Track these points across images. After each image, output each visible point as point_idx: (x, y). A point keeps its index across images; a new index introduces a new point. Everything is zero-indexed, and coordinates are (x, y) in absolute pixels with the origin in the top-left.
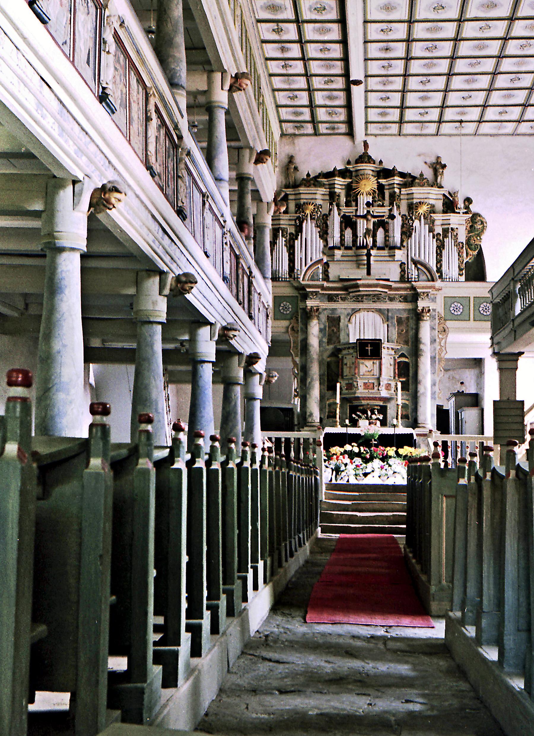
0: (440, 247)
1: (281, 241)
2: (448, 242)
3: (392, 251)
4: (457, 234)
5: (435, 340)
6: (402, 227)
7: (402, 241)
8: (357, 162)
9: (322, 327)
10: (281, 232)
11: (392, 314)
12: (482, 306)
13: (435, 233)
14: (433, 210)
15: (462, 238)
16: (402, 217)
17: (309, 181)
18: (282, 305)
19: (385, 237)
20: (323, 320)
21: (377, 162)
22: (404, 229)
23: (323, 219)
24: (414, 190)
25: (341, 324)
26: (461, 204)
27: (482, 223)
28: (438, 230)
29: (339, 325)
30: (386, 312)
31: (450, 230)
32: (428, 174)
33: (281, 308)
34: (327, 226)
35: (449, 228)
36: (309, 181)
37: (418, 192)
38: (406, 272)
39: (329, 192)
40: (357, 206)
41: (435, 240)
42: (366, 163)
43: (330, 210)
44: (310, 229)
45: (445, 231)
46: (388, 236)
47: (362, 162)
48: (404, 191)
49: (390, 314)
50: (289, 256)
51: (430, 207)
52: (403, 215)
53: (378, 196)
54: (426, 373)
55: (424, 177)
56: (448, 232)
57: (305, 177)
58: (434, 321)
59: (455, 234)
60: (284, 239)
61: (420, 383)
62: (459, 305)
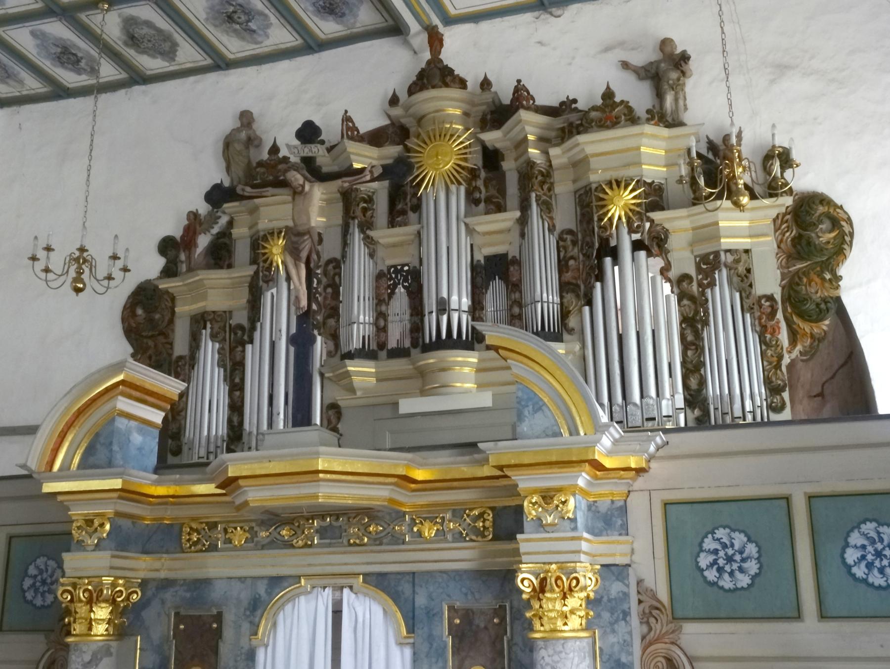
1: (209, 351)
2: (722, 298)
4: (749, 271)
7: (564, 314)
8: (411, 91)
10: (209, 325)
11: (430, 598)
12: (855, 538)
14: (655, 197)
15: (768, 280)
16: (561, 239)
18: (32, 571)
19: (510, 308)
21: (473, 79)
22: (568, 276)
23: (325, 273)
24: (591, 143)
27: (835, 223)
28: (684, 261)
29: (216, 651)
30: (406, 588)
32: (636, 94)
33: (28, 582)
34: (336, 294)
42: (434, 87)
45: (709, 264)
47: (421, 90)
48: (554, 152)
49: (421, 600)
51: (646, 195)
52: (562, 232)
53: (486, 186)
55: (617, 99)
58: (621, 627)
59: (741, 269)
60: (217, 345)
62: (739, 539)
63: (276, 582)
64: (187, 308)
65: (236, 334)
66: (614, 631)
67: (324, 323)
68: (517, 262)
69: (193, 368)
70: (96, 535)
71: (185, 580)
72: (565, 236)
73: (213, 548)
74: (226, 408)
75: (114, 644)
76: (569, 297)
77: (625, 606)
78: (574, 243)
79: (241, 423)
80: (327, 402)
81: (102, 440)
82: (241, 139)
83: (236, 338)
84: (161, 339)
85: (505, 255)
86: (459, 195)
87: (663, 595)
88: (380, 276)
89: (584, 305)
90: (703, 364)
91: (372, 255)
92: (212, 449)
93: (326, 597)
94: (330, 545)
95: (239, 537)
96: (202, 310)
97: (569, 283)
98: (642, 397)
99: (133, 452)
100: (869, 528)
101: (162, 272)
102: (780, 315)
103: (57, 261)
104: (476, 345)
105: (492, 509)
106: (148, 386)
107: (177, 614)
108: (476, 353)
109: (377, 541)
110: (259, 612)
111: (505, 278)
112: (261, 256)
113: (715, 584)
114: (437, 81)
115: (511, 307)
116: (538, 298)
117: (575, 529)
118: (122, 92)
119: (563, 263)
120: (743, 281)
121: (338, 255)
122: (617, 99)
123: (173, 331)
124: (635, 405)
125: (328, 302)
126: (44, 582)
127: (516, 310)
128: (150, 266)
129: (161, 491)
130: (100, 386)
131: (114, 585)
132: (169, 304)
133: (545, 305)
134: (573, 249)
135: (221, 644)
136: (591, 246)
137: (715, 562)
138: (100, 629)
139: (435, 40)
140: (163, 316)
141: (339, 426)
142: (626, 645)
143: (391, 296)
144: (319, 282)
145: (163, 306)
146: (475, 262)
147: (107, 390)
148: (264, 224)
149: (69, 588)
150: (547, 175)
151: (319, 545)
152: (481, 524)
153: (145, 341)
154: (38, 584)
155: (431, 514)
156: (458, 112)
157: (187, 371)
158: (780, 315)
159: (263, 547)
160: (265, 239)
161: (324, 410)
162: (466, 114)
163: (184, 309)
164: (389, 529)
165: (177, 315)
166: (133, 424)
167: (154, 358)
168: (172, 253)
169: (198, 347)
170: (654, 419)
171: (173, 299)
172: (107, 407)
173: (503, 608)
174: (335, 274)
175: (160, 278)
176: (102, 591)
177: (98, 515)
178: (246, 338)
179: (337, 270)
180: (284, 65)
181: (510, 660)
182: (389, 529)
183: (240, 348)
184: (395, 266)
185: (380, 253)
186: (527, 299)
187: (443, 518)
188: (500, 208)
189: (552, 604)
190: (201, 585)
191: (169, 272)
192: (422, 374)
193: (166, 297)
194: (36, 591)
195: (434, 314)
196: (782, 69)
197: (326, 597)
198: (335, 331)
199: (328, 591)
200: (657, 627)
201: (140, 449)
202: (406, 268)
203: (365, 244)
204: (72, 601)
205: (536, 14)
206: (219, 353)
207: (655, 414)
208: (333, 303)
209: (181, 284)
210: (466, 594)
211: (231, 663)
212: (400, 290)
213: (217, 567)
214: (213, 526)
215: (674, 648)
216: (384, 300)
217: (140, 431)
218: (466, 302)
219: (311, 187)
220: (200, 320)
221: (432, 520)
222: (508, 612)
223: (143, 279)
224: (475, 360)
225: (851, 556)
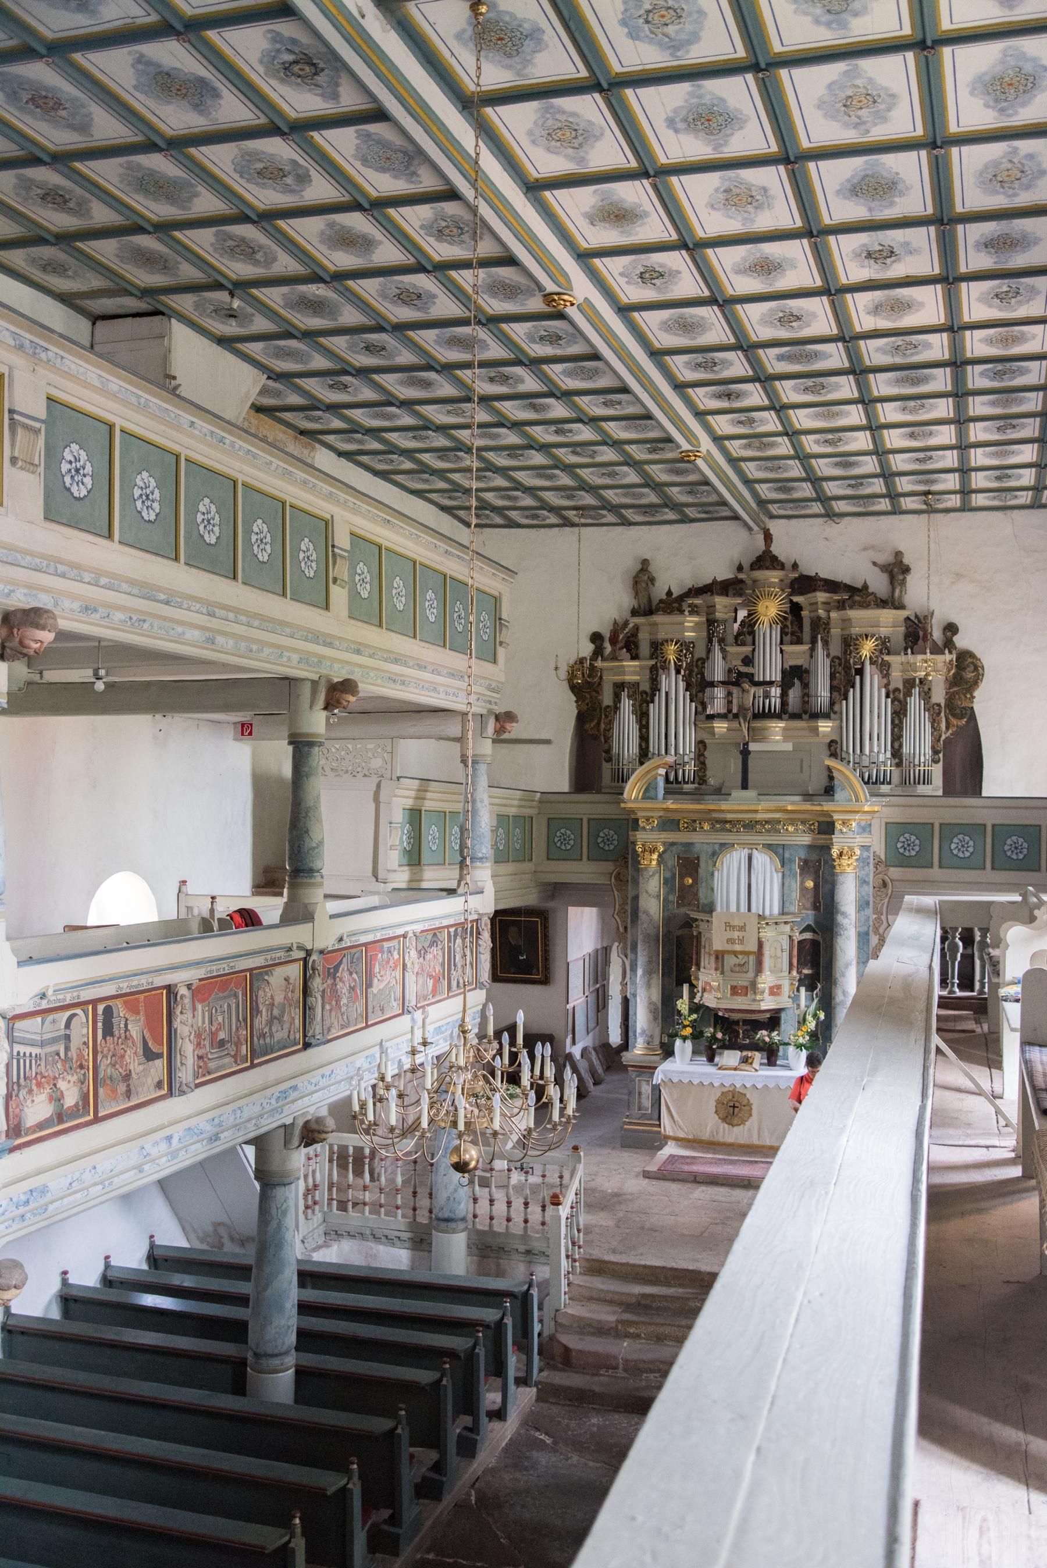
0: (899, 714)
1: (627, 705)
2: (915, 703)
3: (812, 724)
5: (868, 903)
6: (832, 676)
7: (832, 703)
9: (668, 875)
12: (955, 840)
13: (891, 687)
15: (939, 696)
16: (832, 661)
17: (670, 604)
18: (601, 834)
20: (670, 864)
22: (835, 683)
23: (697, 666)
24: (855, 614)
25: (702, 871)
26: (937, 635)
27: (976, 668)
30: (781, 851)
31: (917, 681)
33: (600, 840)
35: (914, 680)
36: (670, 604)
37: (859, 617)
39: (708, 620)
40: (754, 644)
41: (889, 700)
42: (767, 568)
43: (709, 651)
44: (672, 684)
45: (909, 684)
46: (808, 695)
47: (759, 568)
48: (834, 615)
49: (787, 855)
50: (640, 730)
52: (834, 657)
55: (870, 590)
56: (913, 686)
57: (664, 597)
58: (866, 868)
59: (926, 688)
61: (836, 984)
62: (913, 838)
63: (722, 845)
68: (807, 671)
73: (695, 830)
76: (835, 694)
78: (840, 664)
79: (648, 747)
80: (698, 739)
82: (642, 576)
84: (594, 694)
86: (777, 630)
87: (883, 857)
90: (902, 736)
91: (724, 658)
93: (746, 851)
95: (706, 826)
100: (961, 836)
102: (942, 714)
104: (784, 716)
109: (768, 831)
111: (800, 679)
114: (768, 563)
118: (557, 529)
120: (926, 695)
121: (704, 656)
122: (870, 590)
138: (654, 863)
139: (768, 537)
142: (868, 875)
148: (661, 636)
150: (828, 624)
155: (792, 822)
156: (777, 580)
158: (942, 714)
160: (662, 644)
162: (781, 580)
163: (609, 679)
169: (620, 702)
172: (653, 773)
180: (667, 527)
185: (729, 658)
186: (812, 692)
188: (799, 641)
189: (845, 861)
196: (959, 576)
197: (746, 851)
199: (746, 850)
205: (825, 519)
213: (695, 838)
214: (694, 821)
220: (619, 687)
225: (953, 846)
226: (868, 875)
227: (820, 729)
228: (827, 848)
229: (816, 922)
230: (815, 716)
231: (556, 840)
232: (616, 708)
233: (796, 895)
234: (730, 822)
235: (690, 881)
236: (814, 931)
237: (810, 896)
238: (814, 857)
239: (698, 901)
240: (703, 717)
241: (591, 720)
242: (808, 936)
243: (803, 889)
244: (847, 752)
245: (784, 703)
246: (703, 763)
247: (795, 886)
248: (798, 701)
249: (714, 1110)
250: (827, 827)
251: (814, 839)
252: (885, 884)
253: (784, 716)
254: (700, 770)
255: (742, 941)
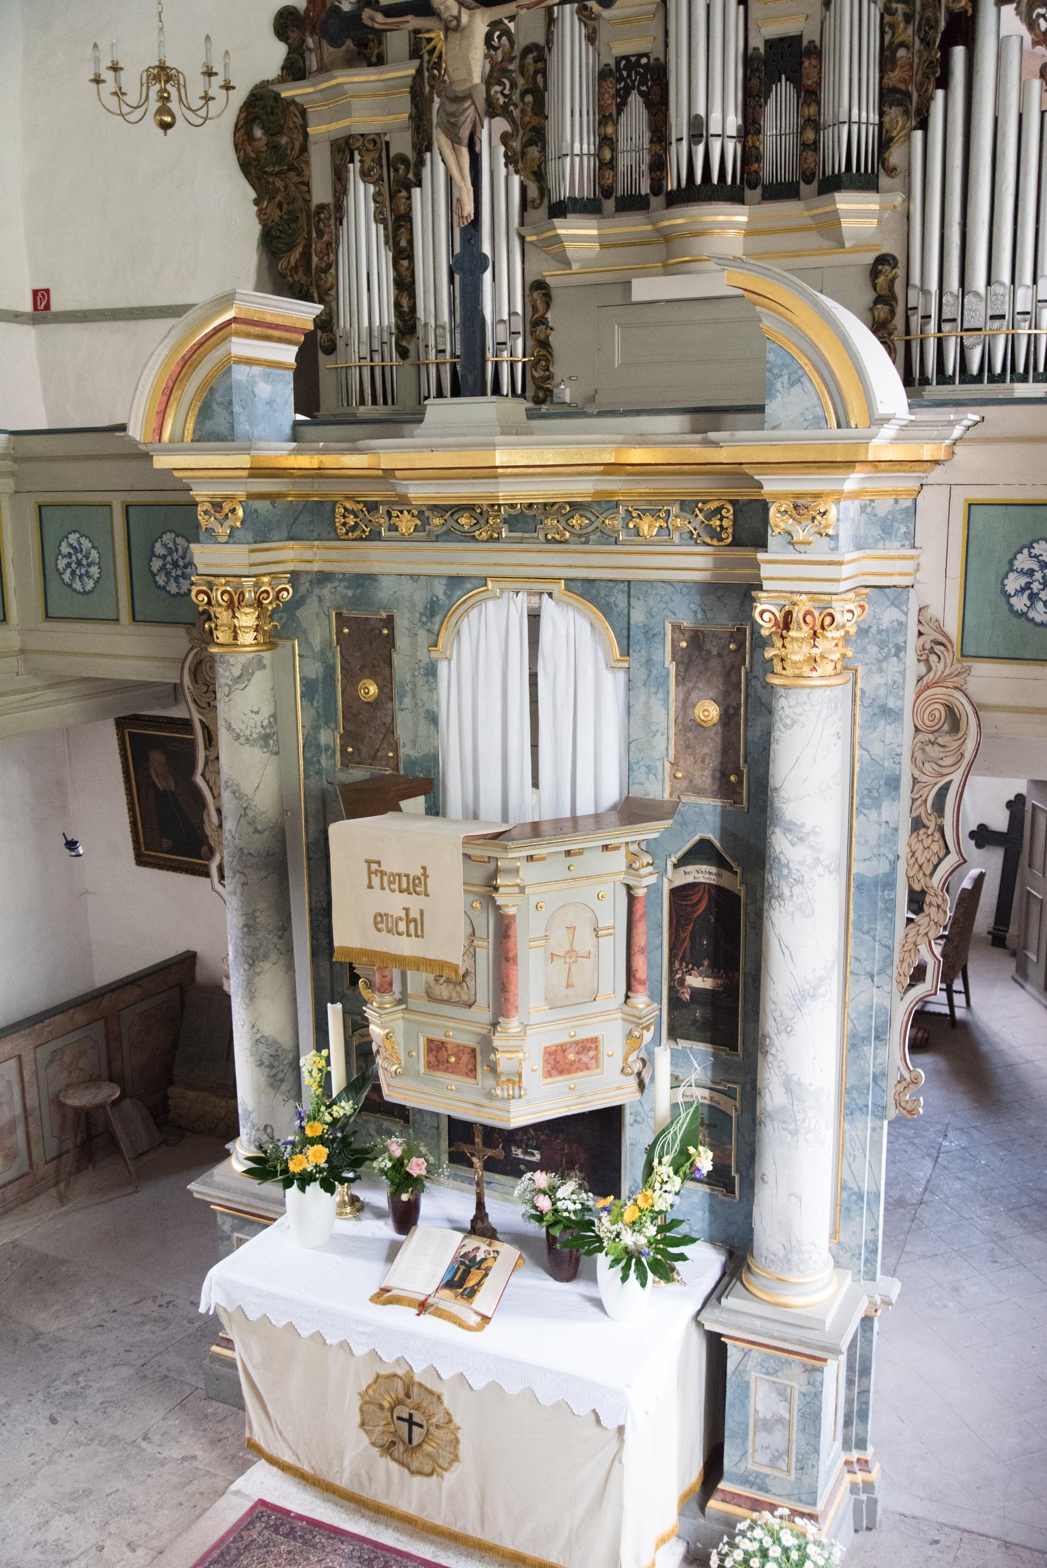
1: (361, 197)
3: (821, 206)
5: (893, 783)
6: (887, 59)
7: (884, 142)
9: (315, 669)
10: (357, 157)
11: (650, 614)
18: (159, 549)
22: (894, 77)
25: (399, 660)
30: (621, 600)
33: (156, 564)
38: (900, 309)
49: (638, 617)
54: (803, 997)
60: (372, 189)
63: (456, 582)
64: (323, 128)
65: (396, 170)
66: (881, 670)
67: (523, 154)
69: (341, 223)
70: (227, 523)
71: (344, 574)
72: (894, 5)
73: (375, 536)
74: (392, 285)
75: (267, 655)
77: (900, 640)
78: (908, 18)
79: (413, 308)
80: (531, 279)
81: (218, 397)
83: (397, 179)
85: (798, 39)
87: (953, 629)
88: (604, 74)
89: (915, 128)
92: (376, 346)
94: (521, 541)
95: (406, 524)
96: (346, 134)
97: (894, 90)
98: (989, 283)
99: (261, 408)
101: (283, 68)
103: (131, 80)
104: (748, 193)
105: (733, 502)
106: (269, 319)
107: (339, 615)
108: (745, 208)
109: (583, 538)
110: (438, 619)
111: (795, 79)
112: (424, 43)
113: (1023, 615)
115: (803, 129)
116: (844, 117)
117: (836, 549)
119: (887, 53)
123: (307, 163)
124: (977, 294)
125: (527, 119)
126: (175, 564)
127: (810, 135)
128: (269, 57)
129: (305, 461)
130: (206, 327)
131: (257, 585)
132: (299, 121)
133: (855, 127)
134: (905, 29)
135: (395, 656)
136: (933, 25)
137: (1028, 586)
138: (247, 638)
140: (292, 142)
141: (549, 315)
142: (895, 688)
143: (620, 108)
144: (513, 85)
145: (291, 124)
146: (750, 51)
147: (216, 330)
149: (204, 588)
151: (510, 540)
152: (718, 523)
153: (270, 179)
154: (169, 566)
157: (333, 227)
159: (437, 539)
161: (527, 292)
163: (321, 130)
164: (597, 524)
165: (311, 139)
166: (256, 370)
167: (285, 206)
168: (294, 35)
169: (345, 191)
170: (1003, 317)
171: (303, 113)
172: (218, 354)
173: (741, 631)
174: (536, 72)
175: (281, 80)
176: (242, 593)
177: (226, 498)
178: (411, 176)
179: (540, 65)
181: (747, 696)
182: (597, 524)
183: (404, 193)
184: (626, 58)
185: (603, 35)
186: (827, 117)
187: (668, 512)
190: (363, 581)
191: (294, 69)
192: (667, 238)
193: (292, 108)
194: (168, 574)
195: (685, 143)
197: (519, 606)
198: (539, 167)
200: (938, 667)
201: (270, 403)
202: (644, 61)
203: (580, 20)
204: (209, 603)
206: (375, 201)
207: (1006, 310)
208: (535, 121)
209: (311, 90)
210: (695, 612)
211: (408, 678)
212: (635, 101)
213: (380, 559)
214: (372, 507)
215: (958, 695)
216: (611, 115)
217: (267, 378)
218: (734, 122)
219: (471, 16)
220: (344, 148)
221: (655, 514)
222: (748, 637)
223: (257, 80)
224: (744, 219)
226: (895, 688)
227: (846, 224)
228: (745, 592)
229: (725, 833)
230: (832, 184)
231: (62, 563)
232: (338, 210)
233: (664, 745)
234: (471, 508)
235: (373, 689)
236: (720, 862)
237: (710, 748)
238: (723, 622)
239: (396, 751)
240: (543, 212)
241: (291, 248)
242: (702, 874)
243: (689, 727)
244: (925, 291)
245: (750, 156)
246: (544, 344)
247: (664, 715)
248: (789, 143)
249: (357, 1419)
250: (747, 526)
251: (718, 564)
252: (954, 721)
253: (748, 193)
254: (535, 364)
255: (416, 925)
